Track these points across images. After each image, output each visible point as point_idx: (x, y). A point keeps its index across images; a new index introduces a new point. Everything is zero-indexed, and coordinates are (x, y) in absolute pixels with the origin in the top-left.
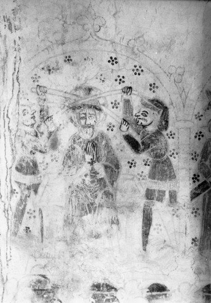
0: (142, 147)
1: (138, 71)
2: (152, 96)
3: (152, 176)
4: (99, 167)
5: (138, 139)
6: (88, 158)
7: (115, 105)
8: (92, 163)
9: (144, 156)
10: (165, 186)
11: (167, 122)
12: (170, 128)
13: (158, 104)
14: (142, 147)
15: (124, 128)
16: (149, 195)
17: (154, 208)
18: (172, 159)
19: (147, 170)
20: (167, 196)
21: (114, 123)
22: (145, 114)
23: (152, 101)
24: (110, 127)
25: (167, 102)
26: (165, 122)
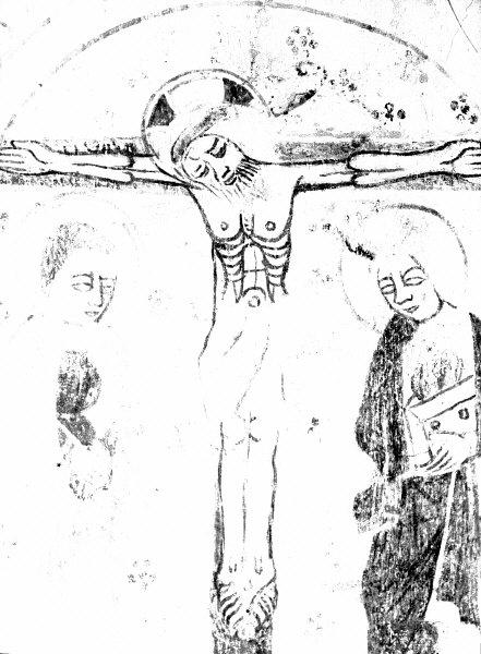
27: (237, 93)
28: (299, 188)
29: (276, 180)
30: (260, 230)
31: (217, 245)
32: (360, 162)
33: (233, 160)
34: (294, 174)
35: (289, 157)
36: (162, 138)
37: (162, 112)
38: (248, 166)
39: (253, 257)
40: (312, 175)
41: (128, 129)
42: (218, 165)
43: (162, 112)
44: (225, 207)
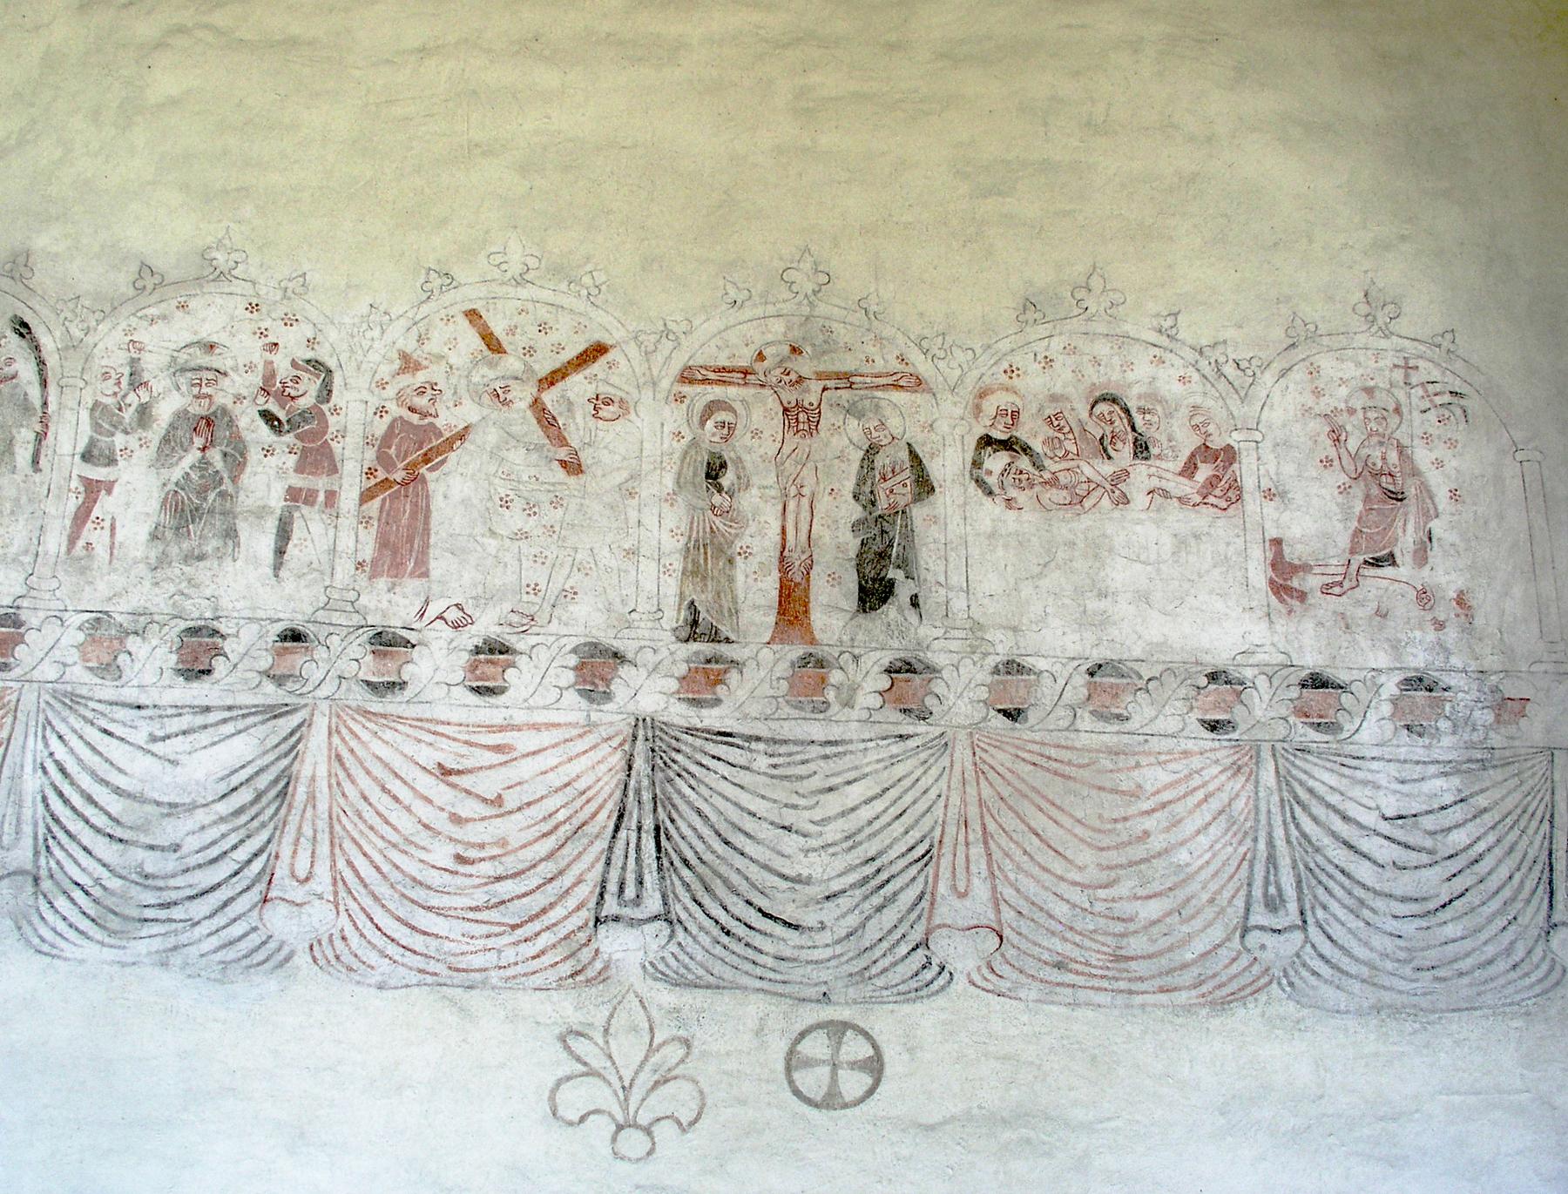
0: (287, 427)
1: (289, 321)
2: (309, 355)
3: (299, 469)
4: (215, 455)
5: (282, 415)
6: (199, 442)
7: (250, 367)
8: (204, 449)
9: (289, 438)
10: (321, 483)
11: (330, 391)
12: (334, 399)
13: (316, 365)
14: (287, 427)
15: (261, 400)
16: (293, 494)
17: (296, 515)
18: (333, 444)
19: (292, 460)
20: (321, 497)
21: (245, 392)
22: (296, 380)
23: (308, 362)
24: (239, 398)
25: (331, 363)
26: (326, 392)
27: (795, 350)
28: (825, 389)
29: (816, 386)
30: (806, 404)
31: (785, 410)
32: (853, 379)
33: (793, 377)
34: (822, 384)
35: (820, 376)
36: (759, 367)
37: (761, 357)
38: (800, 379)
39: (802, 417)
40: (830, 384)
41: (744, 363)
42: (787, 379)
43: (761, 357)
44: (790, 396)
